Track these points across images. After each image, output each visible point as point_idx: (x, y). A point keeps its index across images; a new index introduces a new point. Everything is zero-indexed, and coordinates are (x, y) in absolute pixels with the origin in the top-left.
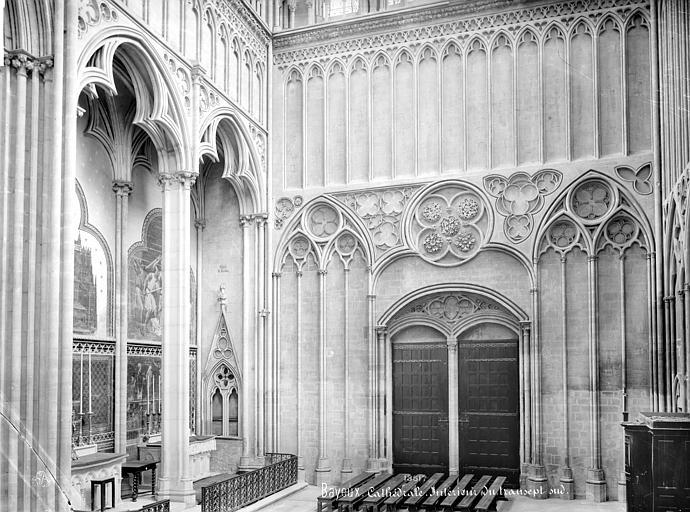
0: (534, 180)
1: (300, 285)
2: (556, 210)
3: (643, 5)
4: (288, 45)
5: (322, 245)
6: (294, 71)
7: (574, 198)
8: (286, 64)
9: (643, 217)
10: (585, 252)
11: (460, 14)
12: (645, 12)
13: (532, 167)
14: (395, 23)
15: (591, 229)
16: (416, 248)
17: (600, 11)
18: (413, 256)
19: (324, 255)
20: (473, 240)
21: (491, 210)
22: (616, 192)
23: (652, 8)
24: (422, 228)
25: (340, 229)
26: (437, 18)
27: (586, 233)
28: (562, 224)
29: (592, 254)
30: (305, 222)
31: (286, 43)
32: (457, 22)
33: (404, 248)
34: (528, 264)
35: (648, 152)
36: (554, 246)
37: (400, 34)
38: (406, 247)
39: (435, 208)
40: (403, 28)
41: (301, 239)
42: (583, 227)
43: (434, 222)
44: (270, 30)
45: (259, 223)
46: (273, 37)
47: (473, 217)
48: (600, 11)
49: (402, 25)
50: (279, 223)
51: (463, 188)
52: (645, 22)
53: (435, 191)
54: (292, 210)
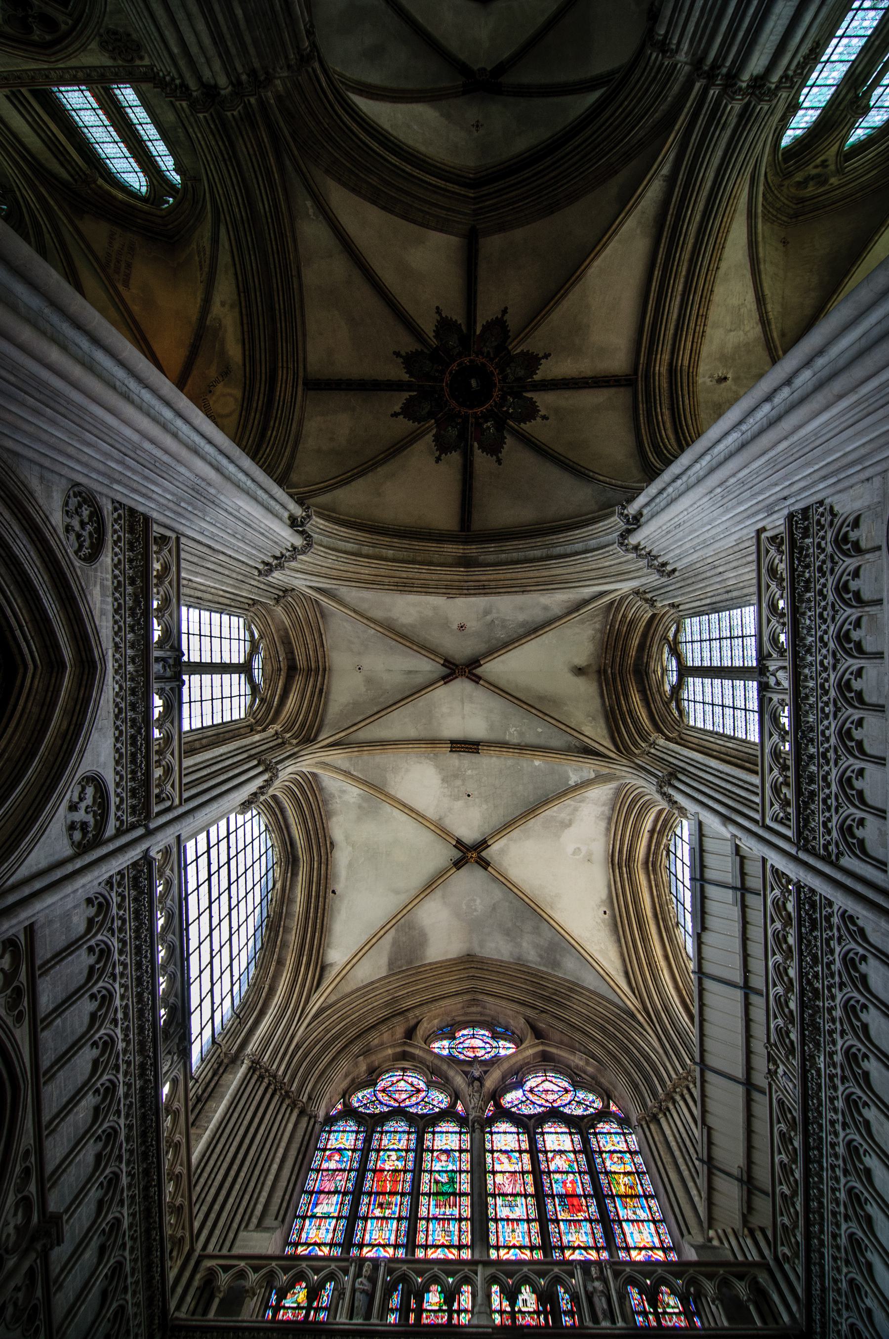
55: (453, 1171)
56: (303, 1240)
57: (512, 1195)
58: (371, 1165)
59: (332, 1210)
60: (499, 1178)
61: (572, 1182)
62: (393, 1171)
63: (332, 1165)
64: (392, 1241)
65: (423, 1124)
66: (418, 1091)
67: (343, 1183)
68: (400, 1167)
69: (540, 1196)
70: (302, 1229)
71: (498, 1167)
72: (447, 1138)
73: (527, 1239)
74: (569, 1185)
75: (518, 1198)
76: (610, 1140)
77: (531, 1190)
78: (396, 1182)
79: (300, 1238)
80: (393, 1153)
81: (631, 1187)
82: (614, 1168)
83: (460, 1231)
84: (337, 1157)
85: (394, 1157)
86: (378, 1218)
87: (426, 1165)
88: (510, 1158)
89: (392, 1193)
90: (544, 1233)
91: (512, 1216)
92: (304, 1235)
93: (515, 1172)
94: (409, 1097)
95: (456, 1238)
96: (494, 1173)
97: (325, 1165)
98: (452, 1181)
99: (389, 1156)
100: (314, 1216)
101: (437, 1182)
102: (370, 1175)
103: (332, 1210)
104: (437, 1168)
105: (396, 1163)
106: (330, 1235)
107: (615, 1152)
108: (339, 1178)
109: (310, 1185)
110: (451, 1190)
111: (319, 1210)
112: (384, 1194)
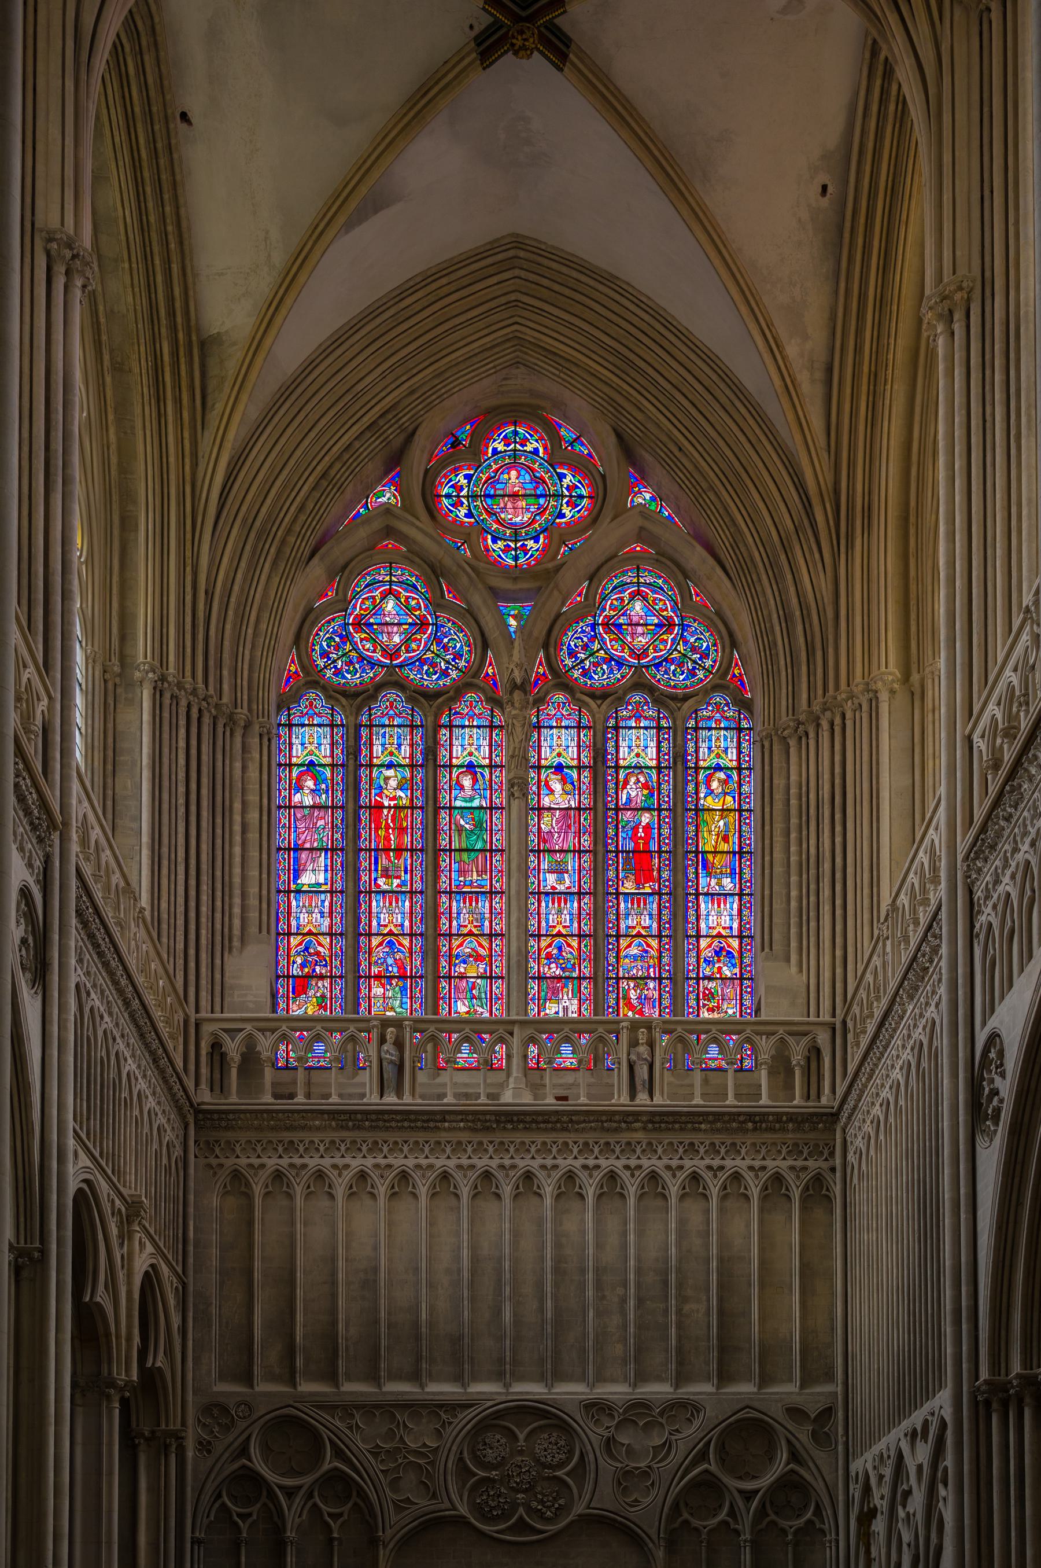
0: (662, 1414)
1: (243, 1559)
2: (694, 1464)
3: (825, 1165)
4: (227, 1128)
5: (290, 1493)
6: (236, 1175)
7: (722, 1448)
8: (222, 1161)
9: (821, 1483)
10: (737, 1533)
11: (546, 1130)
12: (828, 1176)
13: (659, 1390)
14: (431, 1124)
15: (748, 1496)
16: (463, 1510)
17: (764, 1163)
18: (460, 1521)
19: (294, 1515)
20: (562, 1502)
21: (591, 1456)
22: (784, 1443)
23: (838, 1174)
24: (475, 1474)
25: (326, 1466)
26: (505, 1128)
27: (740, 1503)
28: (707, 1488)
29: (748, 1536)
30: (254, 1450)
31: (224, 1124)
32: (539, 1141)
33: (443, 1506)
34: (651, 1545)
35: (828, 1388)
36: (692, 1520)
37: (439, 1143)
38: (447, 1504)
39: (496, 1447)
40: (443, 1134)
41: (249, 1482)
42: (736, 1494)
43: (495, 1467)
44: (196, 1100)
45: (167, 1447)
46: (197, 1112)
47: (561, 1465)
48: (764, 1163)
49: (445, 1129)
50: (204, 1446)
51: (544, 1414)
52: (828, 1190)
53: (499, 1415)
54: (227, 1428)
55: (481, 808)
56: (294, 930)
57: (561, 851)
58: (364, 801)
59: (322, 881)
60: (547, 823)
61: (648, 828)
62: (396, 807)
63: (308, 801)
64: (407, 931)
65: (433, 707)
66: (423, 624)
67: (328, 832)
68: (405, 802)
69: (600, 852)
70: (289, 913)
71: (546, 802)
72: (469, 744)
73: (576, 925)
74: (641, 833)
75: (570, 856)
76: (718, 747)
77: (586, 842)
78: (402, 831)
79: (289, 926)
80: (390, 773)
81: (726, 839)
82: (710, 802)
83: (491, 913)
84: (310, 783)
85: (393, 783)
86: (384, 892)
87: (444, 799)
88: (564, 781)
89: (399, 851)
90: (598, 915)
91: (561, 888)
92: (294, 923)
93: (570, 808)
94: (406, 642)
95: (487, 923)
96: (540, 809)
97: (297, 798)
98: (478, 825)
99: (387, 779)
100: (298, 892)
101: (460, 829)
102: (365, 816)
103: (322, 881)
104: (458, 803)
105: (400, 793)
106: (327, 922)
107: (718, 768)
108: (321, 823)
109: (283, 838)
110: (479, 846)
111: (307, 879)
112: (387, 850)
